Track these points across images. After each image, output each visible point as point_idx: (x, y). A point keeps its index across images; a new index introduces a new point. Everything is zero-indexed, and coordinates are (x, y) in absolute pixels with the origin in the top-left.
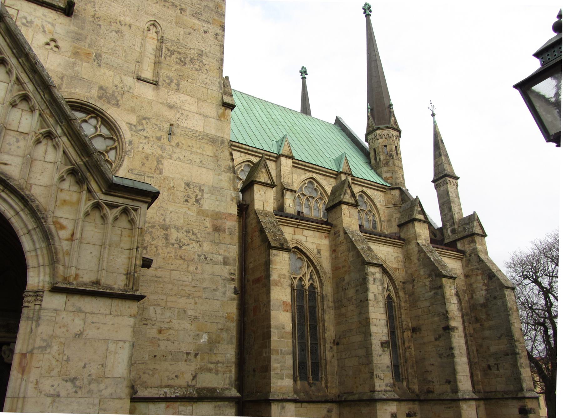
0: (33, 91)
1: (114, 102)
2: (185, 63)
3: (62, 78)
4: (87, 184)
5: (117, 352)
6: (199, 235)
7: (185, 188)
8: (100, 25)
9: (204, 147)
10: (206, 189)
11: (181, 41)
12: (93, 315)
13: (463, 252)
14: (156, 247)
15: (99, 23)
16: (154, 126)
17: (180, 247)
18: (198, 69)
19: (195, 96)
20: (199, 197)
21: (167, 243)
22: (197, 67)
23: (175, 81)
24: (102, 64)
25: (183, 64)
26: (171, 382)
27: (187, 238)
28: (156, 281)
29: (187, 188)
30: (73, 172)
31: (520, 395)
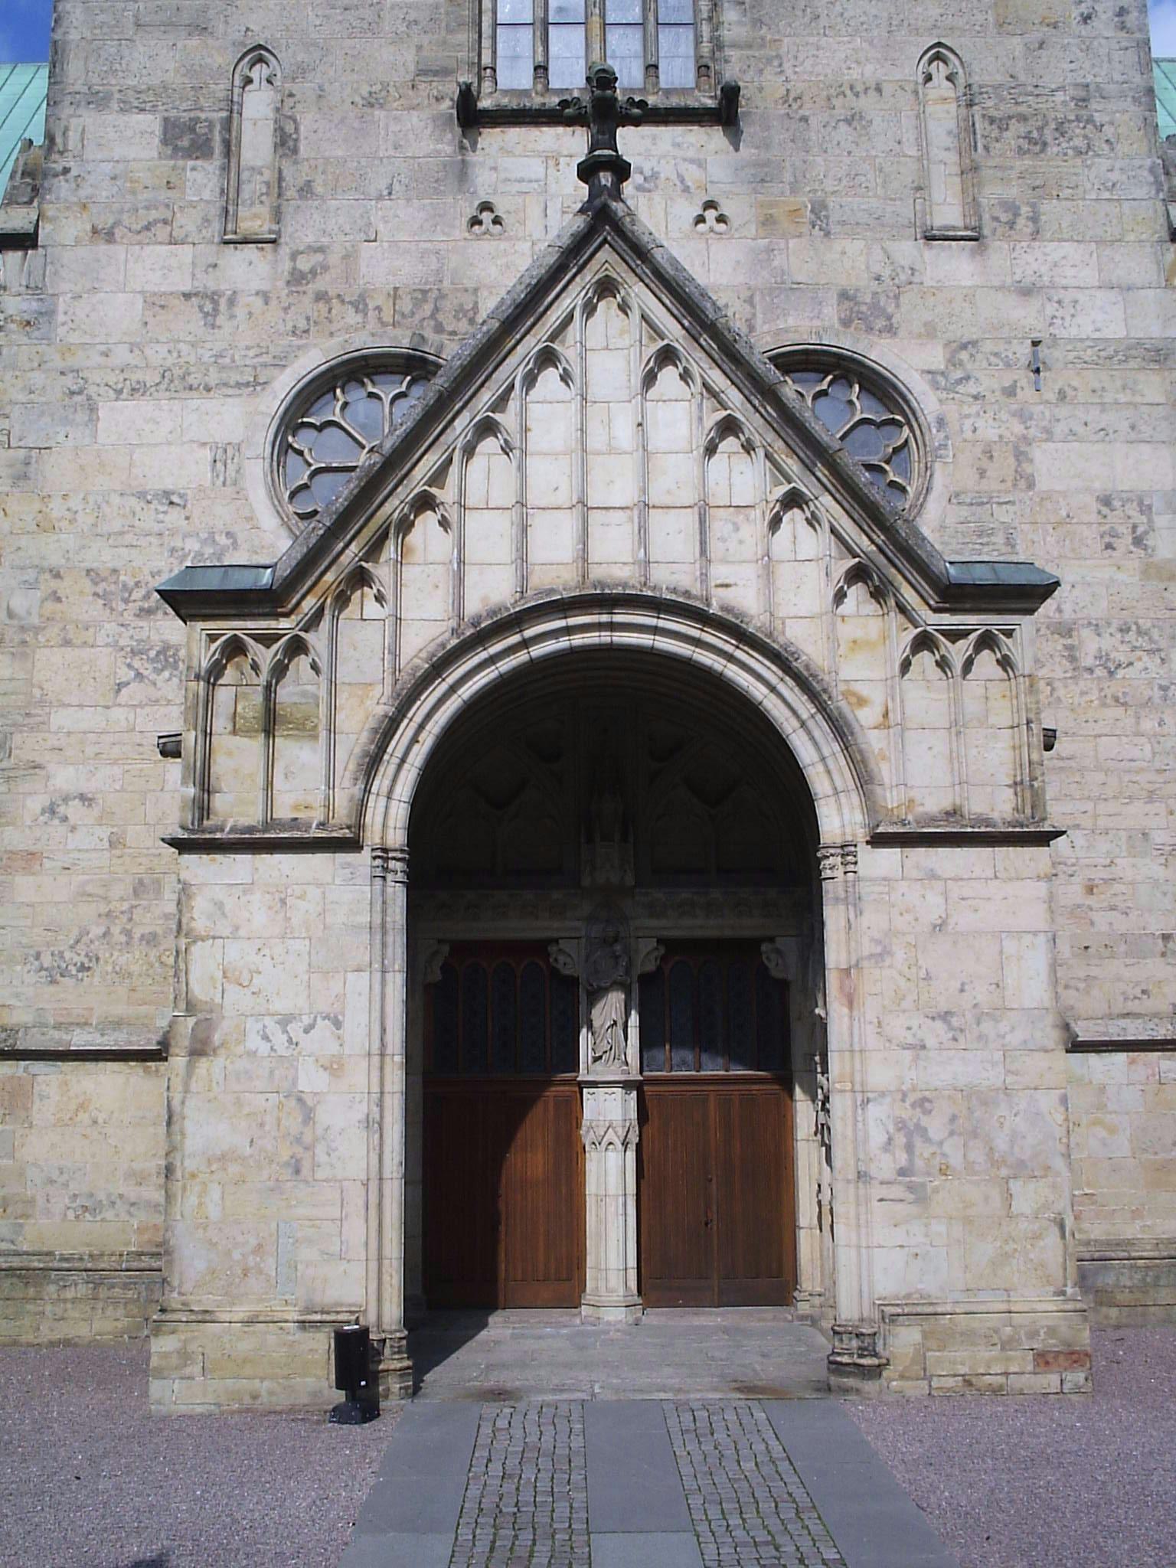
0: (742, 404)
1: (880, 323)
2: (1045, 144)
3: (750, 301)
4: (895, 595)
5: (1022, 957)
6: (1156, 636)
7: (1099, 512)
8: (804, 119)
9: (1135, 382)
10: (1157, 504)
11: (1022, 78)
12: (960, 883)
14: (1048, 684)
15: (801, 112)
16: (993, 359)
17: (1111, 673)
18: (1084, 150)
19: (1088, 238)
20: (1140, 530)
21: (1074, 669)
22: (1079, 142)
23: (1025, 210)
24: (835, 229)
25: (1038, 148)
26: (1133, 1006)
27: (1125, 648)
28: (1062, 768)
29: (1105, 510)
30: (858, 574)
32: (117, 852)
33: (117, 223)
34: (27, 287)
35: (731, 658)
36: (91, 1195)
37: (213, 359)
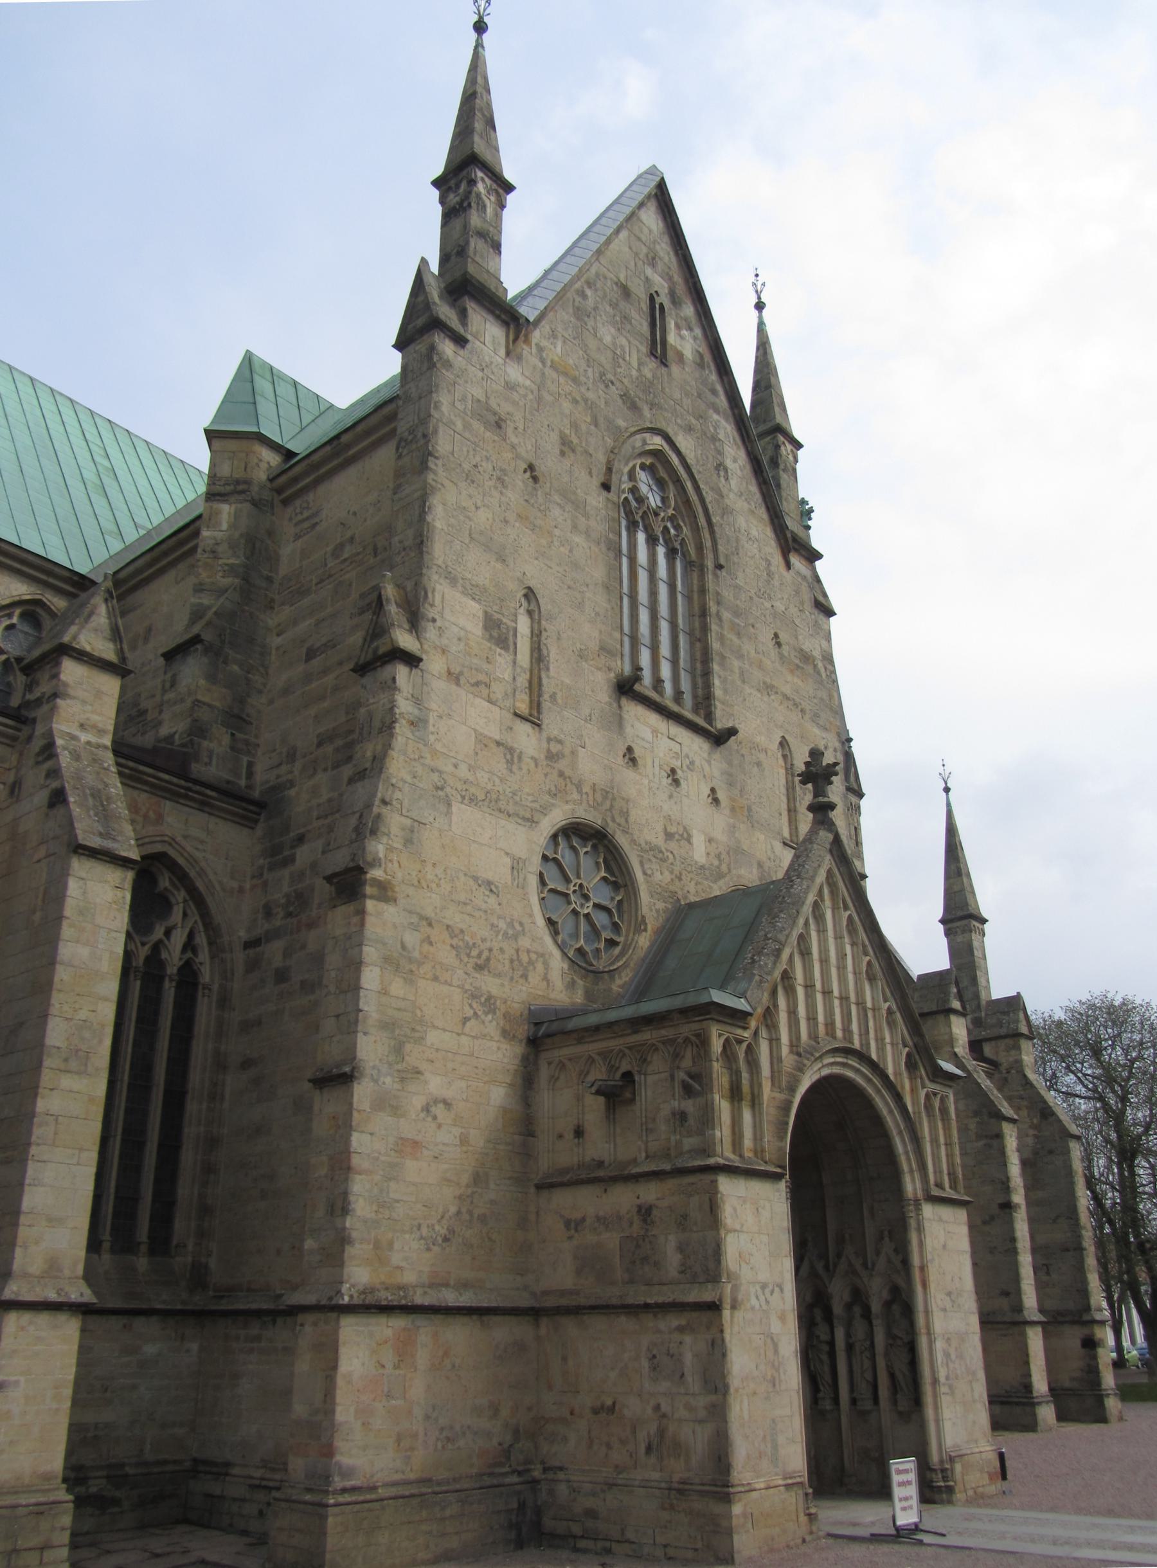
8: (743, 756)
13: (994, 1064)
31: (1086, 1318)
32: (464, 1149)
33: (461, 673)
34: (412, 696)
35: (878, 1091)
36: (451, 1428)
37: (511, 795)
